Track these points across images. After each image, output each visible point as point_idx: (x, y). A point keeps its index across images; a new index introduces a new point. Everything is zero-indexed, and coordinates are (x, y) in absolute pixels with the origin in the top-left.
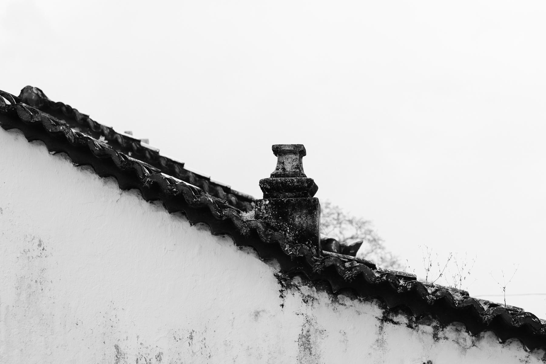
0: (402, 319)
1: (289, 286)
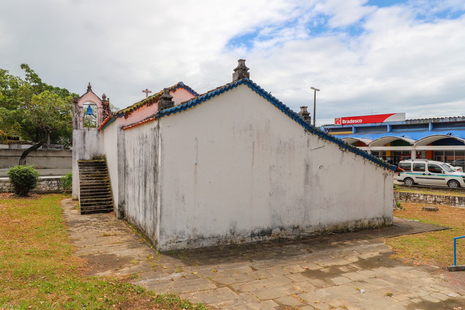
0: (321, 138)
1: (306, 132)
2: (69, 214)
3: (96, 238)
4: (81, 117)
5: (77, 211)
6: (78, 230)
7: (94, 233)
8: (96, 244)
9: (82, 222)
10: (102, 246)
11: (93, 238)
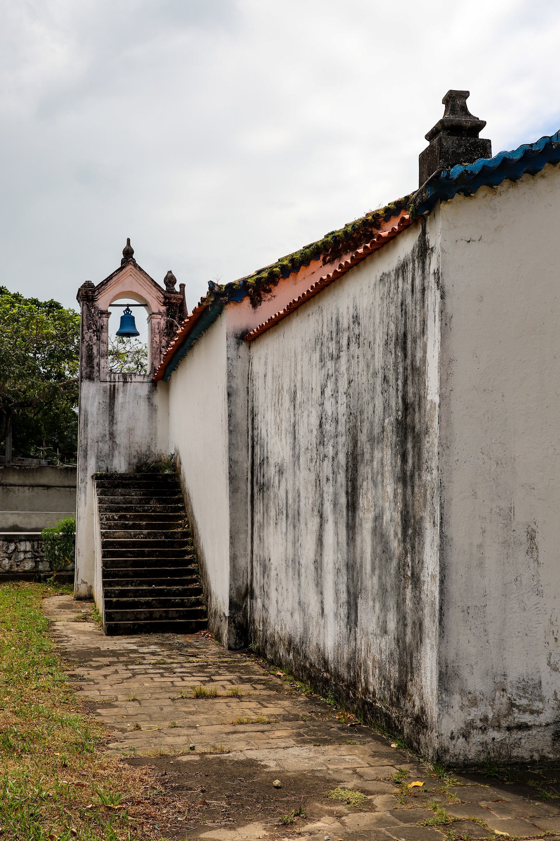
2: (69, 631)
3: (172, 703)
4: (103, 342)
5: (92, 625)
6: (105, 676)
7: (162, 688)
8: (177, 722)
9: (113, 653)
10: (201, 729)
11: (158, 703)
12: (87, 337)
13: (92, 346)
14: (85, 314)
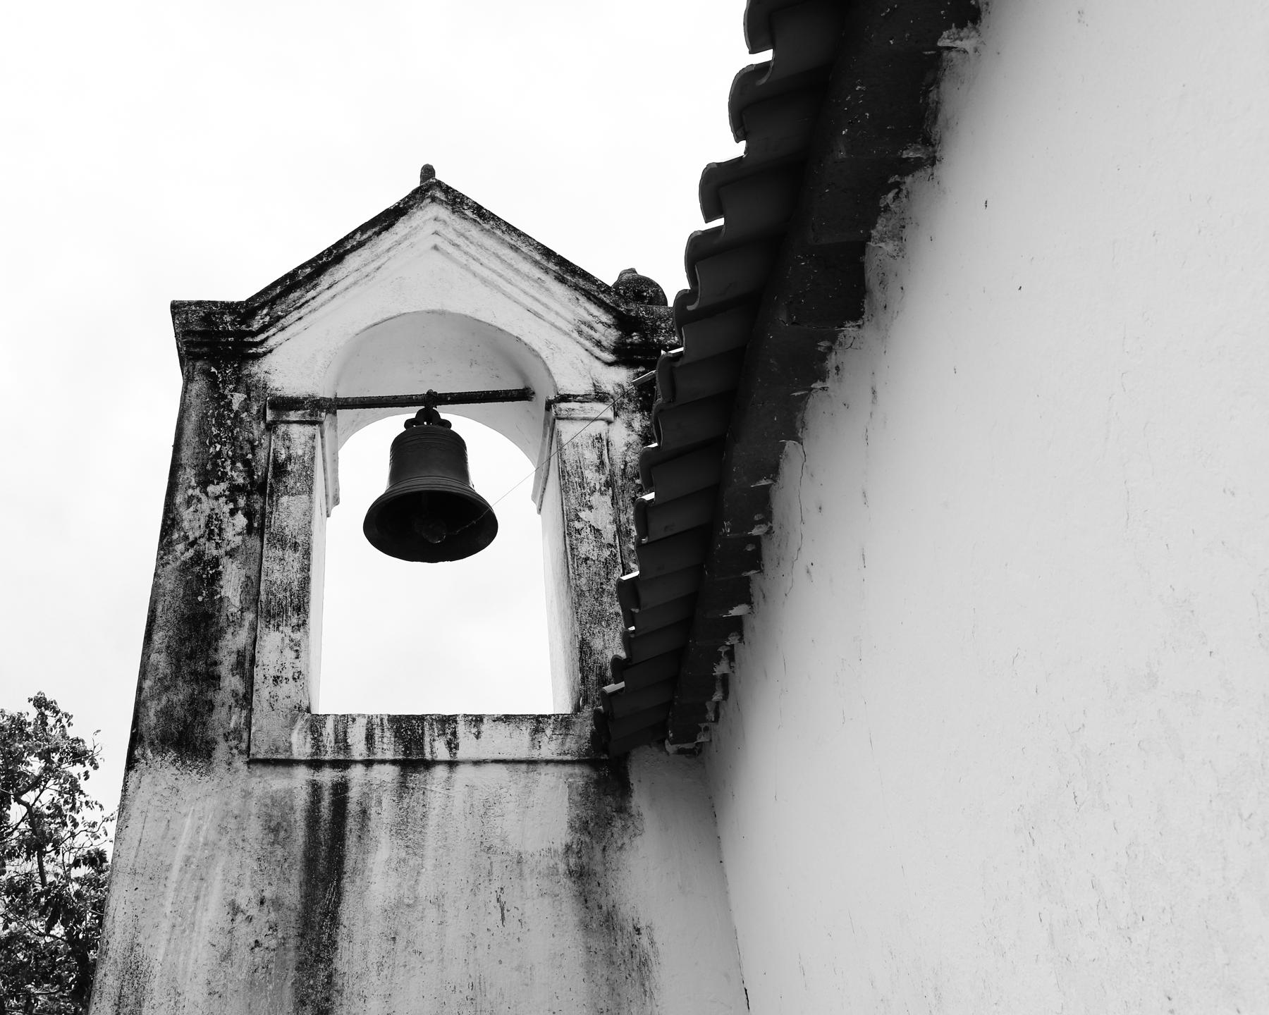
4: (281, 541)
12: (192, 522)
13: (216, 562)
14: (194, 417)
